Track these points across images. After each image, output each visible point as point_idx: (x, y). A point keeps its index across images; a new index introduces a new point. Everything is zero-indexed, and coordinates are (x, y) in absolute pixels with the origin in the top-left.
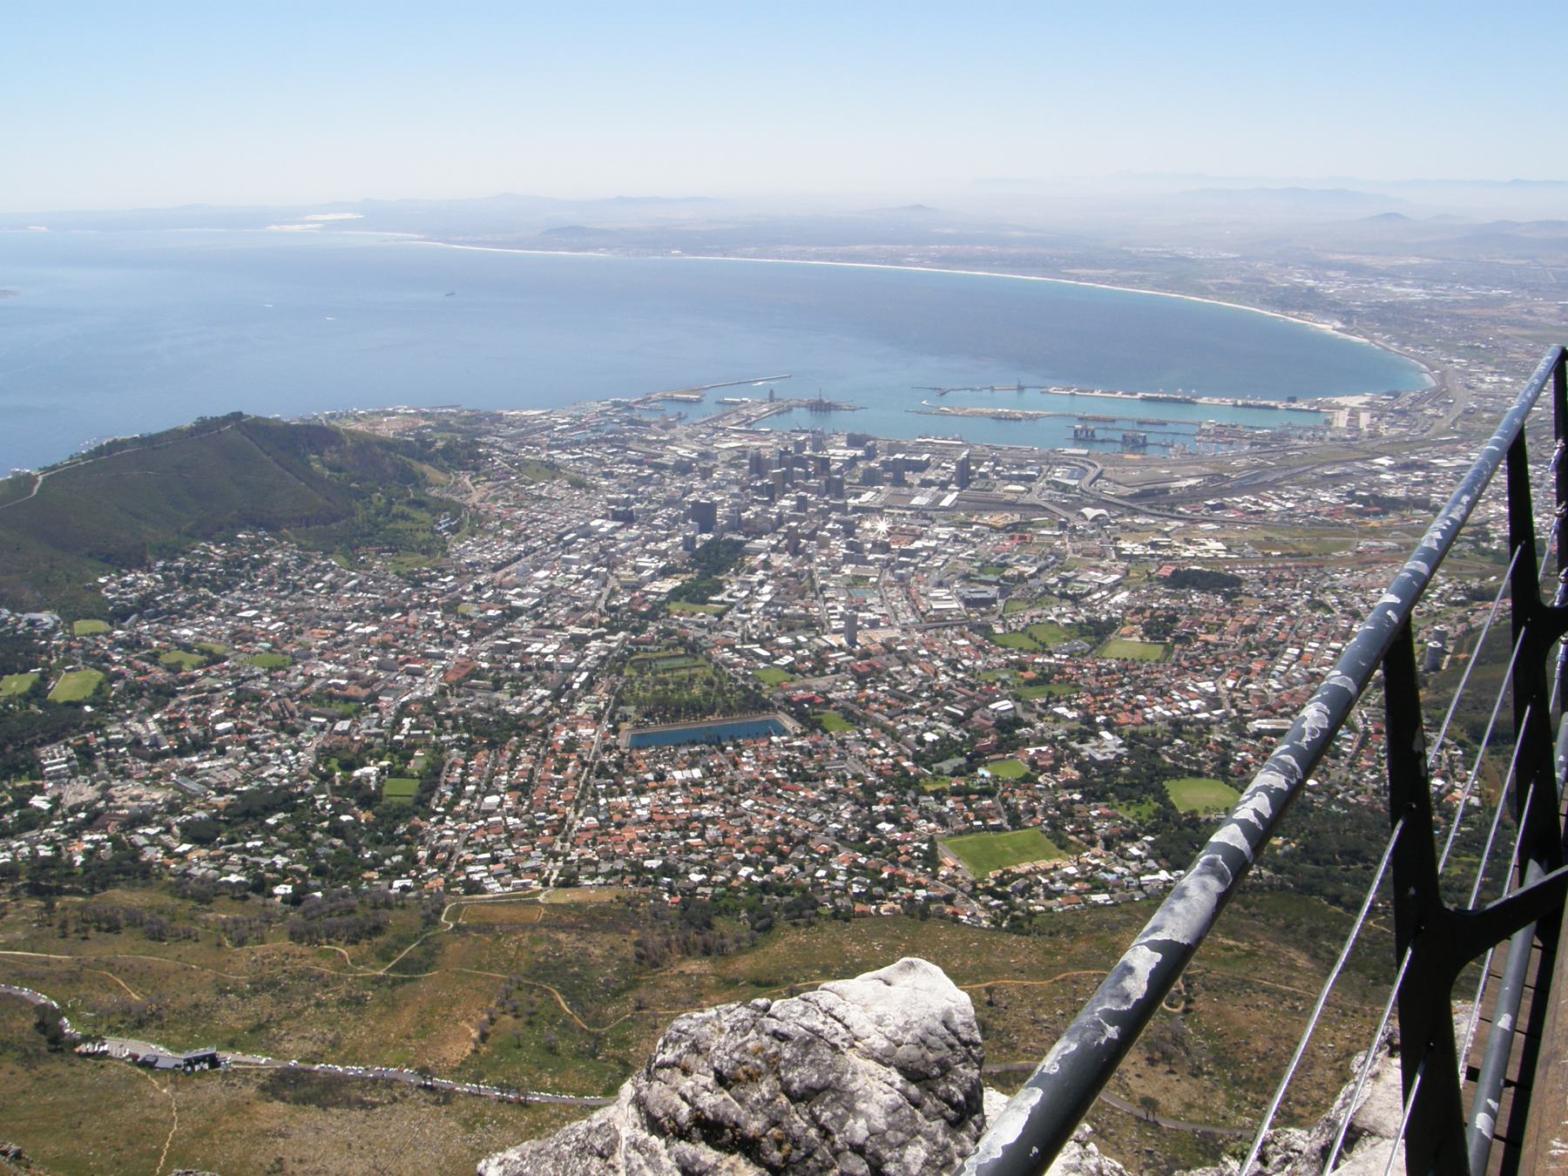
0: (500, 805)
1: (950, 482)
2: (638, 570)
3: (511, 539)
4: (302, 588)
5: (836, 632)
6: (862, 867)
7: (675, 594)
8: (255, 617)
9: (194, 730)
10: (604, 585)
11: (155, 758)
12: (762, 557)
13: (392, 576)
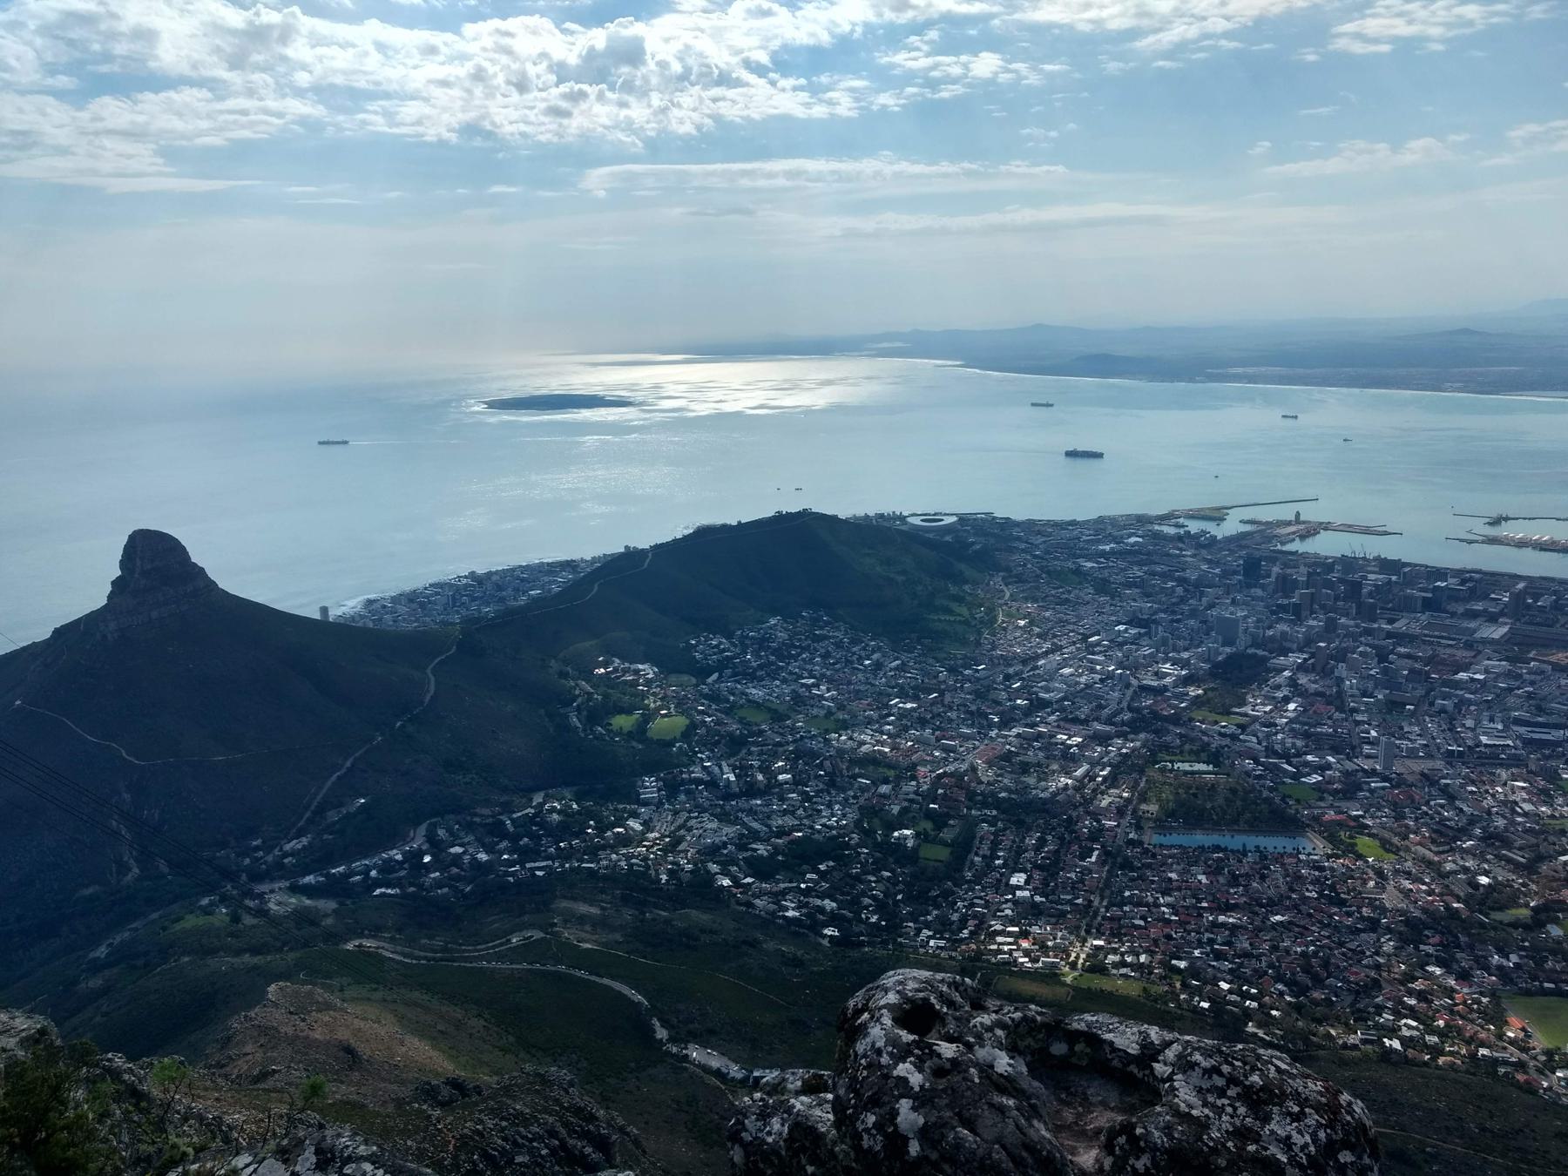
0: (1027, 882)
1: (1502, 614)
2: (1159, 675)
4: (852, 662)
5: (1368, 757)
6: (1411, 1008)
7: (1197, 702)
8: (813, 685)
9: (760, 777)
11: (728, 796)
12: (1287, 673)
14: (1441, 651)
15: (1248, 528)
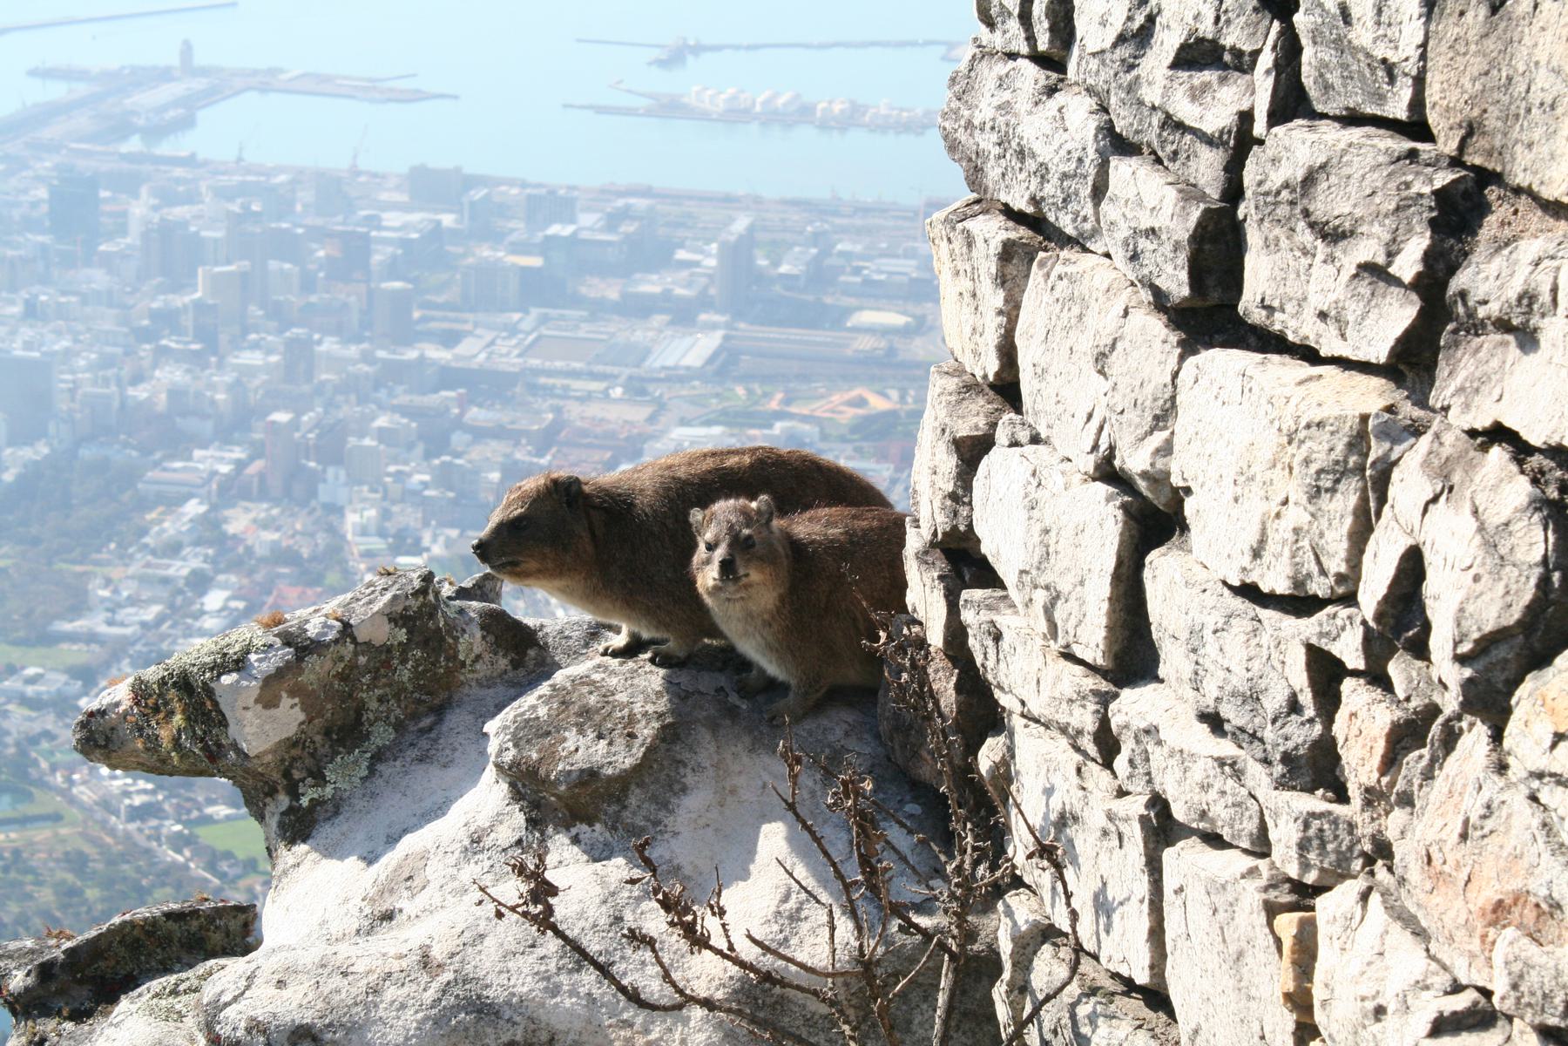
12: (194, 508)
14: (574, 411)
15: (57, 91)
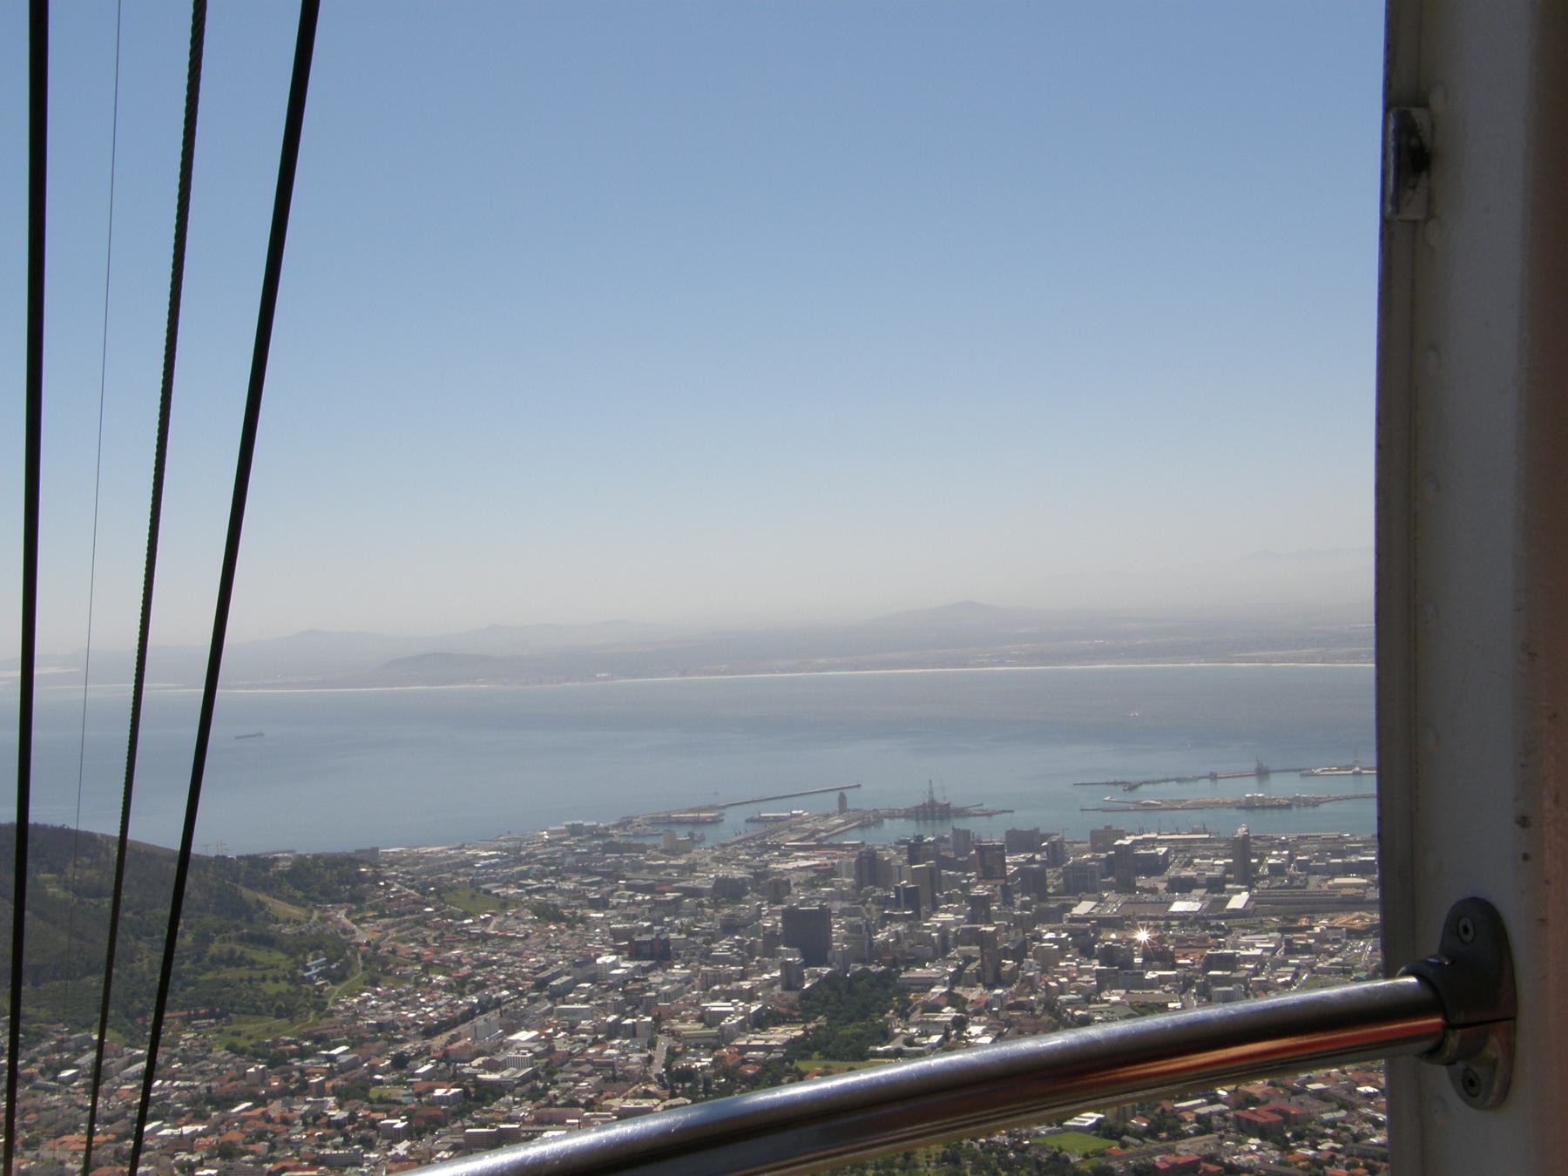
3: (448, 988)
10: (652, 1044)
13: (220, 1052)
